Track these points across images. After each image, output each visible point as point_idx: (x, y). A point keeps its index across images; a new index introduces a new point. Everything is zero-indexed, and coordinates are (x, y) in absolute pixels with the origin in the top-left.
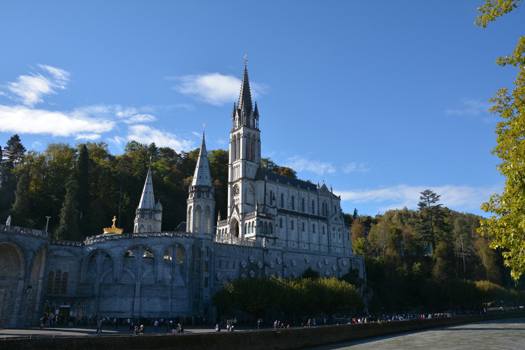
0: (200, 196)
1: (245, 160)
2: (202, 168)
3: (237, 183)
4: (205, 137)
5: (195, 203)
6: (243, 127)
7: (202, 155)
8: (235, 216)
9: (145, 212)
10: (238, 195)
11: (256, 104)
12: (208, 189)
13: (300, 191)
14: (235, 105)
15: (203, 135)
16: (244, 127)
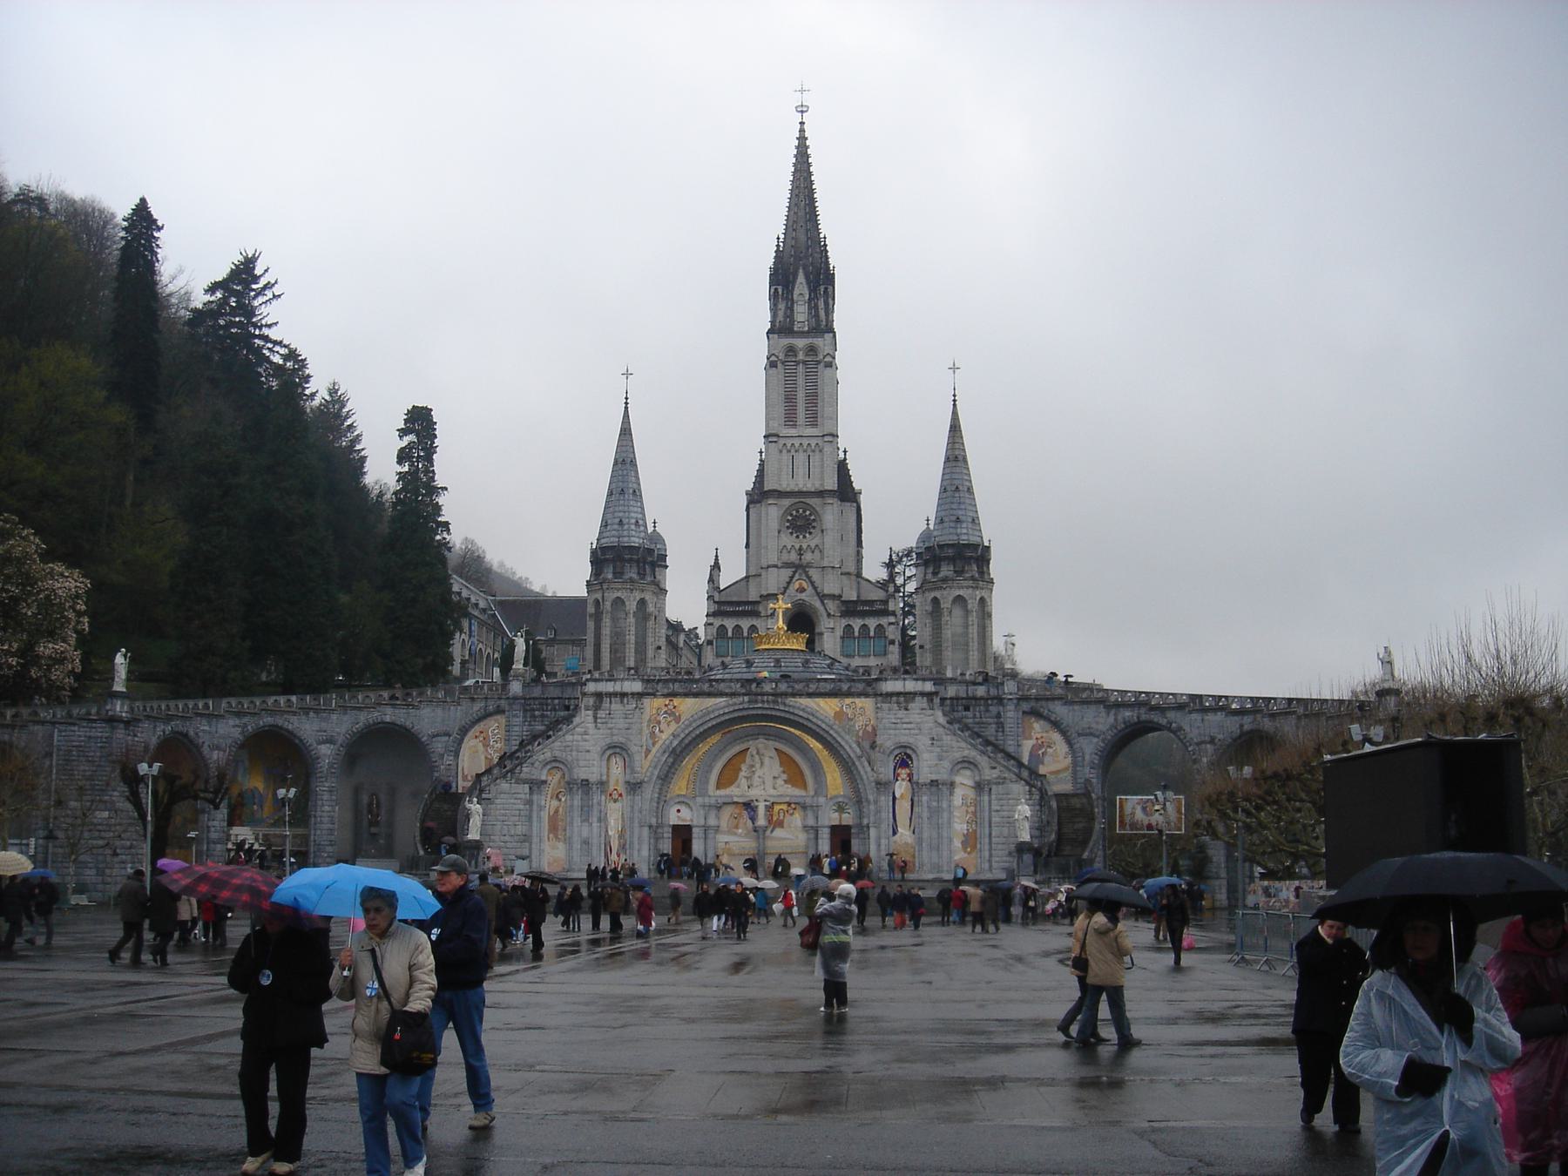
8: (806, 599)
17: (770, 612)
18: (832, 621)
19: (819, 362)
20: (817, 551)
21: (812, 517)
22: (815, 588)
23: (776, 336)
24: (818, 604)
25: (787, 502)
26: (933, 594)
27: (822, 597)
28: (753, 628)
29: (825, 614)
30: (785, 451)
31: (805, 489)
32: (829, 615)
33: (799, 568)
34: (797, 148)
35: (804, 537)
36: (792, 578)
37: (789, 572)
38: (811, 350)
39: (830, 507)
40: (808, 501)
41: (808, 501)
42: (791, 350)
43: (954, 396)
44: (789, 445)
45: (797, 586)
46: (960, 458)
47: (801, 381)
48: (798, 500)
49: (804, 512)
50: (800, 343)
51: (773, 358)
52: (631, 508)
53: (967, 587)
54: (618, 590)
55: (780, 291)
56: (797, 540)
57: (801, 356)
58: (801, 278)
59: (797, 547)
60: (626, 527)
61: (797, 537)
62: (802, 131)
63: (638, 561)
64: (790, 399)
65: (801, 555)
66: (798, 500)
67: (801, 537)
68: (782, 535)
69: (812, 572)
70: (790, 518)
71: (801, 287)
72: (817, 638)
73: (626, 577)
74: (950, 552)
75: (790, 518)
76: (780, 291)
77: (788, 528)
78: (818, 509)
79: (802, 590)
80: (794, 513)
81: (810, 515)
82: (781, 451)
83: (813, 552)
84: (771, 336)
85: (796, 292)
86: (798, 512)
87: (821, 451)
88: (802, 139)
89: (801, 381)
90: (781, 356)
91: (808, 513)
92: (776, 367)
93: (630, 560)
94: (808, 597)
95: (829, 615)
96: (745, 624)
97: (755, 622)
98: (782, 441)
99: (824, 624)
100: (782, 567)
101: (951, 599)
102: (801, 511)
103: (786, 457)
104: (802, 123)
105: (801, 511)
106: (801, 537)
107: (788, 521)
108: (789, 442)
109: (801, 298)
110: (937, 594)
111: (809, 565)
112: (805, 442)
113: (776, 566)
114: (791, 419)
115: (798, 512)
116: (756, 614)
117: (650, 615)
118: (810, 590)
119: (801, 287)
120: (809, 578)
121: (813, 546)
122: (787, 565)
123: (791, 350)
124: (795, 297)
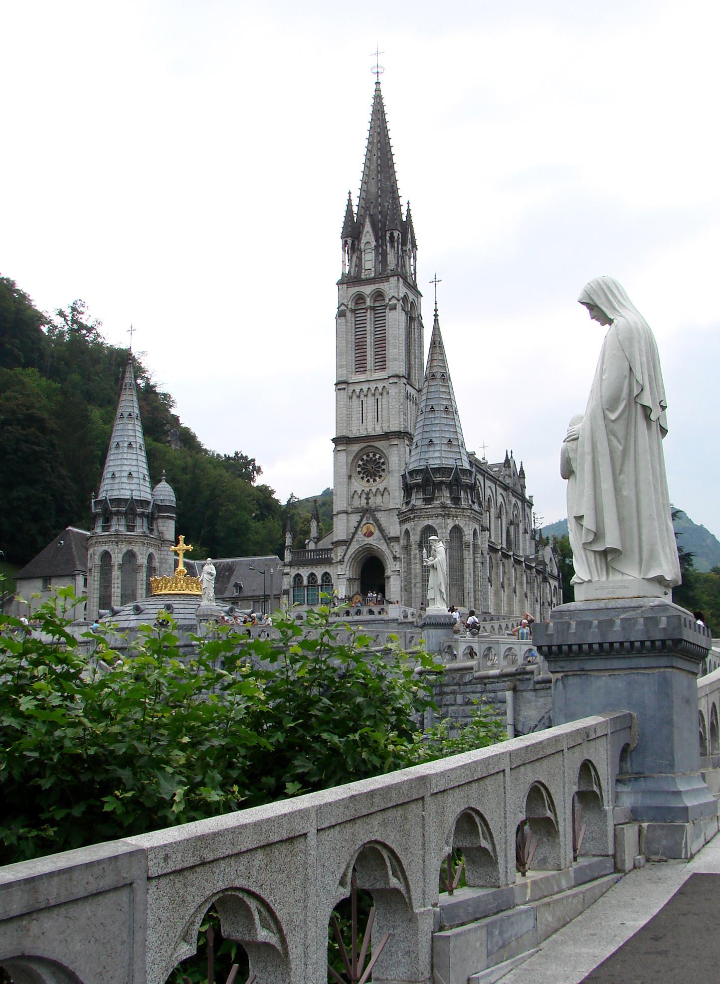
0: (459, 499)
1: (405, 381)
2: (448, 415)
3: (372, 444)
4: (438, 318)
5: (449, 521)
6: (396, 278)
7: (443, 376)
9: (139, 510)
10: (375, 480)
11: (409, 210)
12: (473, 482)
13: (486, 480)
14: (350, 200)
15: (434, 313)
16: (400, 278)
17: (339, 558)
18: (398, 564)
19: (386, 306)
20: (386, 494)
21: (382, 461)
22: (381, 530)
23: (345, 286)
24: (383, 547)
25: (356, 448)
27: (390, 540)
28: (326, 576)
29: (392, 557)
30: (354, 397)
31: (373, 433)
32: (395, 558)
33: (367, 512)
34: (374, 106)
35: (375, 480)
36: (360, 522)
37: (355, 518)
38: (377, 297)
39: (395, 448)
40: (376, 444)
41: (376, 444)
42: (360, 298)
43: (436, 310)
44: (358, 391)
45: (365, 530)
46: (438, 376)
47: (369, 327)
48: (365, 444)
49: (374, 455)
50: (368, 290)
51: (343, 308)
52: (126, 462)
53: (437, 516)
54: (106, 542)
56: (367, 485)
57: (369, 302)
58: (368, 227)
59: (367, 490)
60: (117, 481)
61: (368, 481)
62: (378, 90)
63: (126, 514)
64: (360, 346)
65: (368, 499)
66: (365, 444)
68: (353, 480)
69: (379, 515)
70: (360, 463)
71: (368, 236)
72: (386, 581)
73: (113, 529)
74: (419, 480)
75: (360, 463)
77: (359, 473)
78: (385, 451)
79: (370, 534)
80: (365, 457)
81: (380, 458)
82: (351, 398)
83: (382, 495)
84: (341, 286)
85: (364, 241)
86: (368, 456)
88: (378, 99)
89: (369, 327)
90: (351, 305)
91: (378, 456)
92: (345, 316)
93: (118, 513)
94: (375, 541)
95: (395, 558)
96: (319, 572)
98: (351, 388)
99: (391, 567)
100: (352, 513)
101: (419, 529)
102: (371, 455)
103: (356, 403)
105: (371, 455)
107: (359, 466)
108: (357, 388)
109: (368, 246)
111: (377, 510)
112: (373, 386)
113: (346, 512)
114: (360, 366)
115: (368, 456)
116: (328, 562)
117: (141, 566)
118: (377, 533)
119: (368, 236)
120: (376, 521)
121: (382, 489)
122: (356, 511)
123: (360, 298)
124: (362, 246)
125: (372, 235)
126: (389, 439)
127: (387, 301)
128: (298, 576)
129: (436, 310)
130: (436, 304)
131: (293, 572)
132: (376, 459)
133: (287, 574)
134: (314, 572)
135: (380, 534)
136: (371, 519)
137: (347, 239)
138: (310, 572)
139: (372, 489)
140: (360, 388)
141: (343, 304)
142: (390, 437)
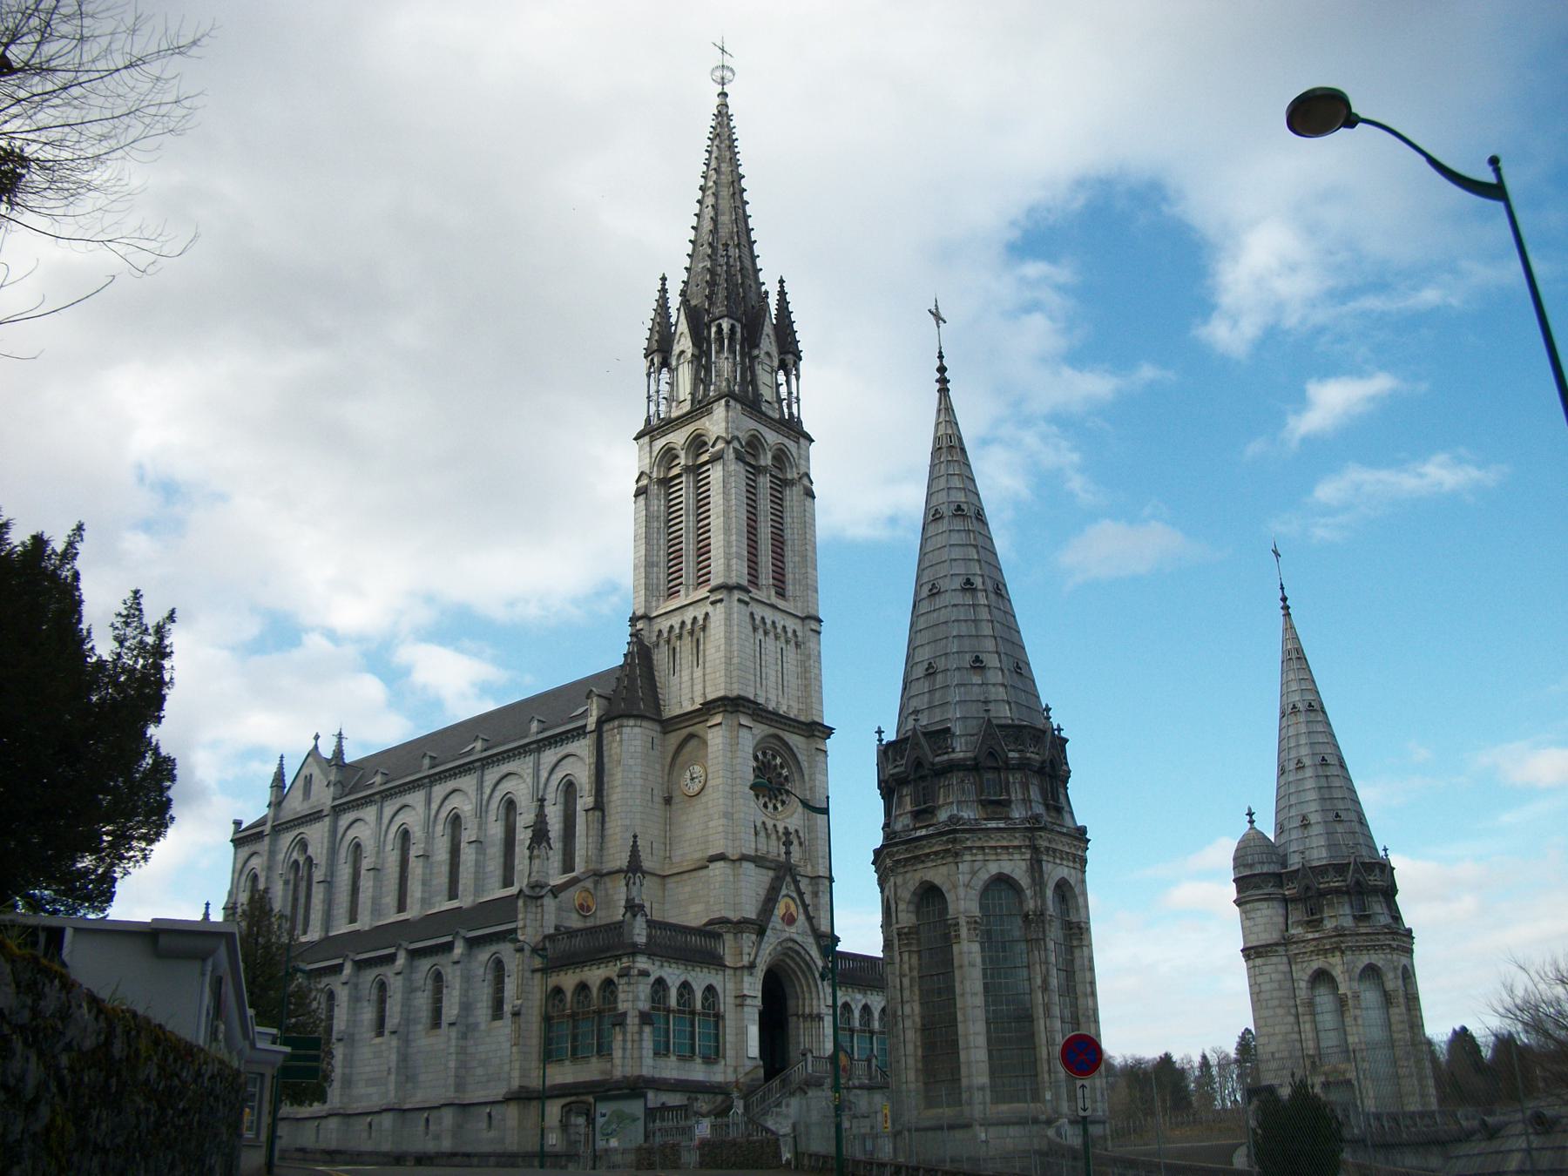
3: (781, 733)
8: (799, 939)
17: (746, 960)
21: (785, 772)
23: (739, 406)
25: (761, 730)
26: (1365, 959)
43: (1284, 599)
48: (772, 731)
55: (739, 330)
65: (788, 843)
66: (772, 731)
67: (770, 806)
76: (739, 330)
79: (790, 920)
81: (782, 767)
87: (797, 645)
88: (723, 115)
91: (778, 761)
96: (700, 979)
97: (715, 979)
104: (724, 95)
106: (770, 806)
110: (1377, 959)
118: (802, 918)
122: (758, 860)
125: (773, 343)
126: (814, 736)
127: (791, 474)
128: (660, 982)
129: (1284, 599)
130: (1282, 588)
131: (656, 971)
132: (776, 765)
133: (645, 973)
134: (690, 979)
135: (807, 924)
136: (793, 887)
137: (736, 324)
138: (682, 978)
139: (778, 824)
140: (761, 614)
141: (738, 438)
142: (817, 733)
